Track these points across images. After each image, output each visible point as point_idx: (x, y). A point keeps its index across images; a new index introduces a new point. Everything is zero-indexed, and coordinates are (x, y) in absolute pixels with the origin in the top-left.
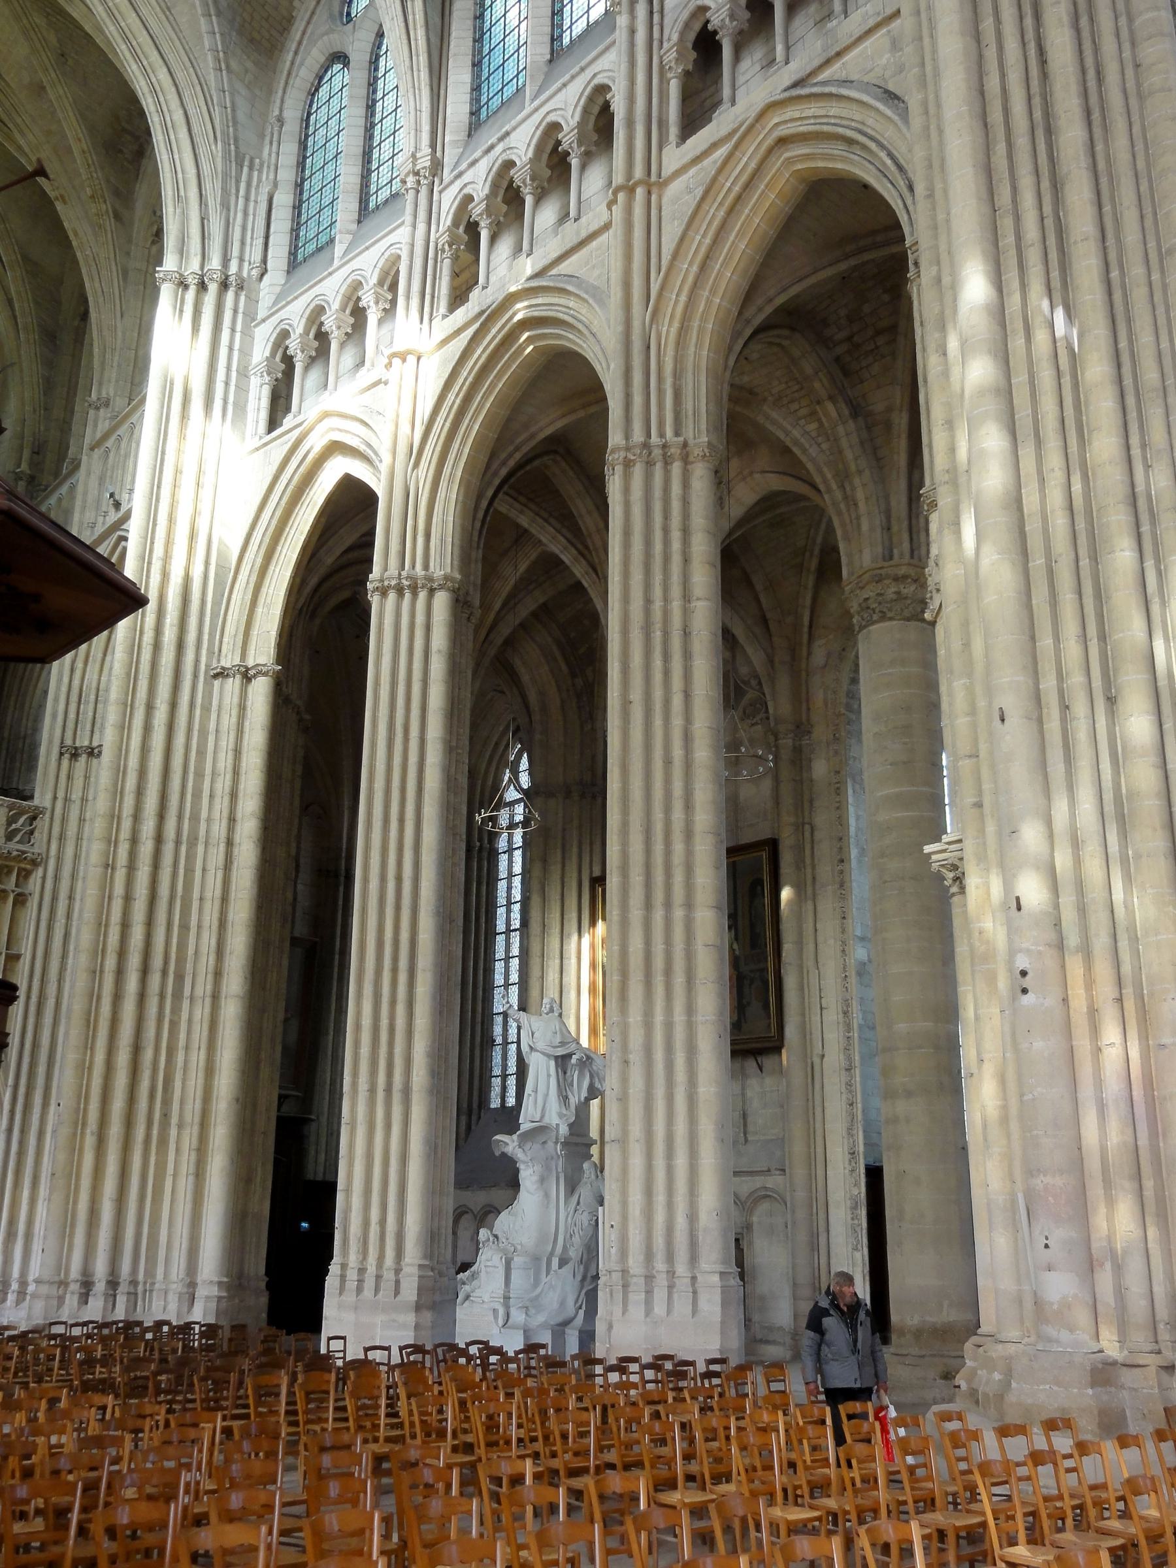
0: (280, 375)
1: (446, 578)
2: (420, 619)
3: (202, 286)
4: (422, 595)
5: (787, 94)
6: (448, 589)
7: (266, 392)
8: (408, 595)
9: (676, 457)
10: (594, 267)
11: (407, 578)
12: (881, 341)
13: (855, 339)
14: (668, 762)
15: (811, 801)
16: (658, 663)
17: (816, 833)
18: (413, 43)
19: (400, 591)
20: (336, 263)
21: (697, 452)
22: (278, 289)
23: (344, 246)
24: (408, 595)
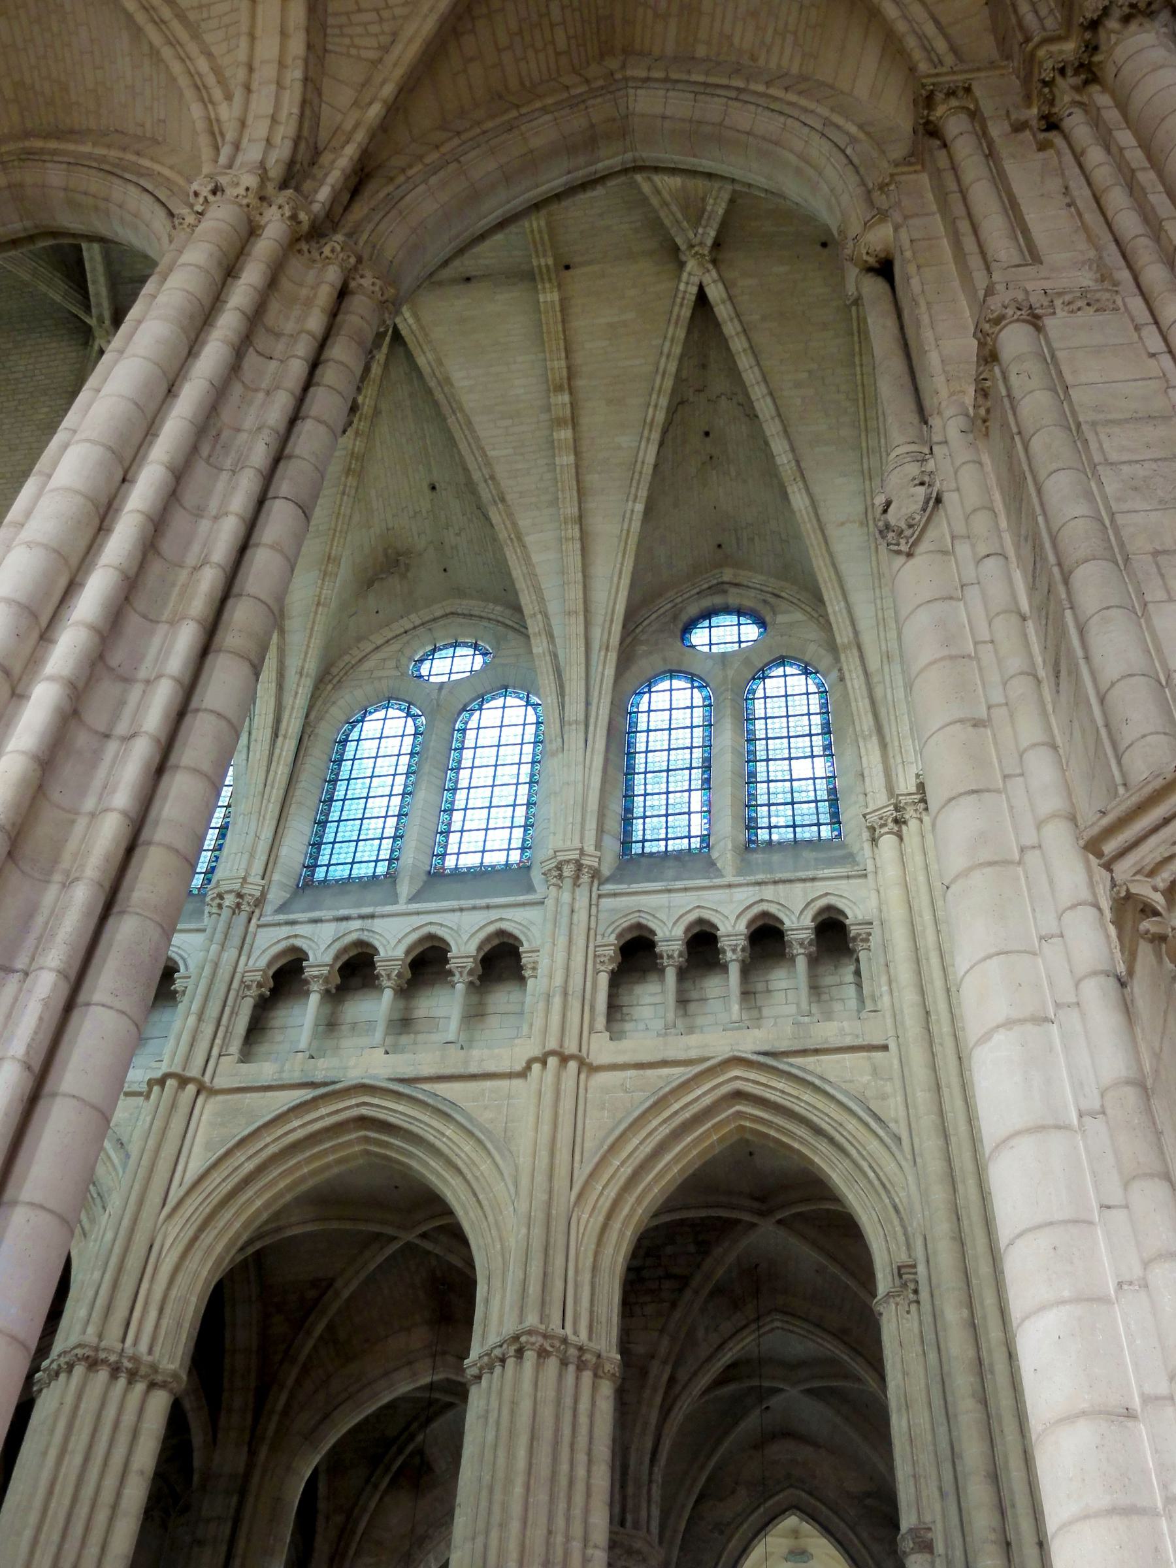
1: (175, 1376)
2: (129, 1418)
4: (140, 1387)
5: (755, 1057)
6: (171, 1391)
9: (590, 1365)
10: (486, 1108)
11: (130, 1359)
12: (667, 1284)
18: (271, 773)
19: (115, 1371)
21: (608, 1367)
24: (122, 1381)
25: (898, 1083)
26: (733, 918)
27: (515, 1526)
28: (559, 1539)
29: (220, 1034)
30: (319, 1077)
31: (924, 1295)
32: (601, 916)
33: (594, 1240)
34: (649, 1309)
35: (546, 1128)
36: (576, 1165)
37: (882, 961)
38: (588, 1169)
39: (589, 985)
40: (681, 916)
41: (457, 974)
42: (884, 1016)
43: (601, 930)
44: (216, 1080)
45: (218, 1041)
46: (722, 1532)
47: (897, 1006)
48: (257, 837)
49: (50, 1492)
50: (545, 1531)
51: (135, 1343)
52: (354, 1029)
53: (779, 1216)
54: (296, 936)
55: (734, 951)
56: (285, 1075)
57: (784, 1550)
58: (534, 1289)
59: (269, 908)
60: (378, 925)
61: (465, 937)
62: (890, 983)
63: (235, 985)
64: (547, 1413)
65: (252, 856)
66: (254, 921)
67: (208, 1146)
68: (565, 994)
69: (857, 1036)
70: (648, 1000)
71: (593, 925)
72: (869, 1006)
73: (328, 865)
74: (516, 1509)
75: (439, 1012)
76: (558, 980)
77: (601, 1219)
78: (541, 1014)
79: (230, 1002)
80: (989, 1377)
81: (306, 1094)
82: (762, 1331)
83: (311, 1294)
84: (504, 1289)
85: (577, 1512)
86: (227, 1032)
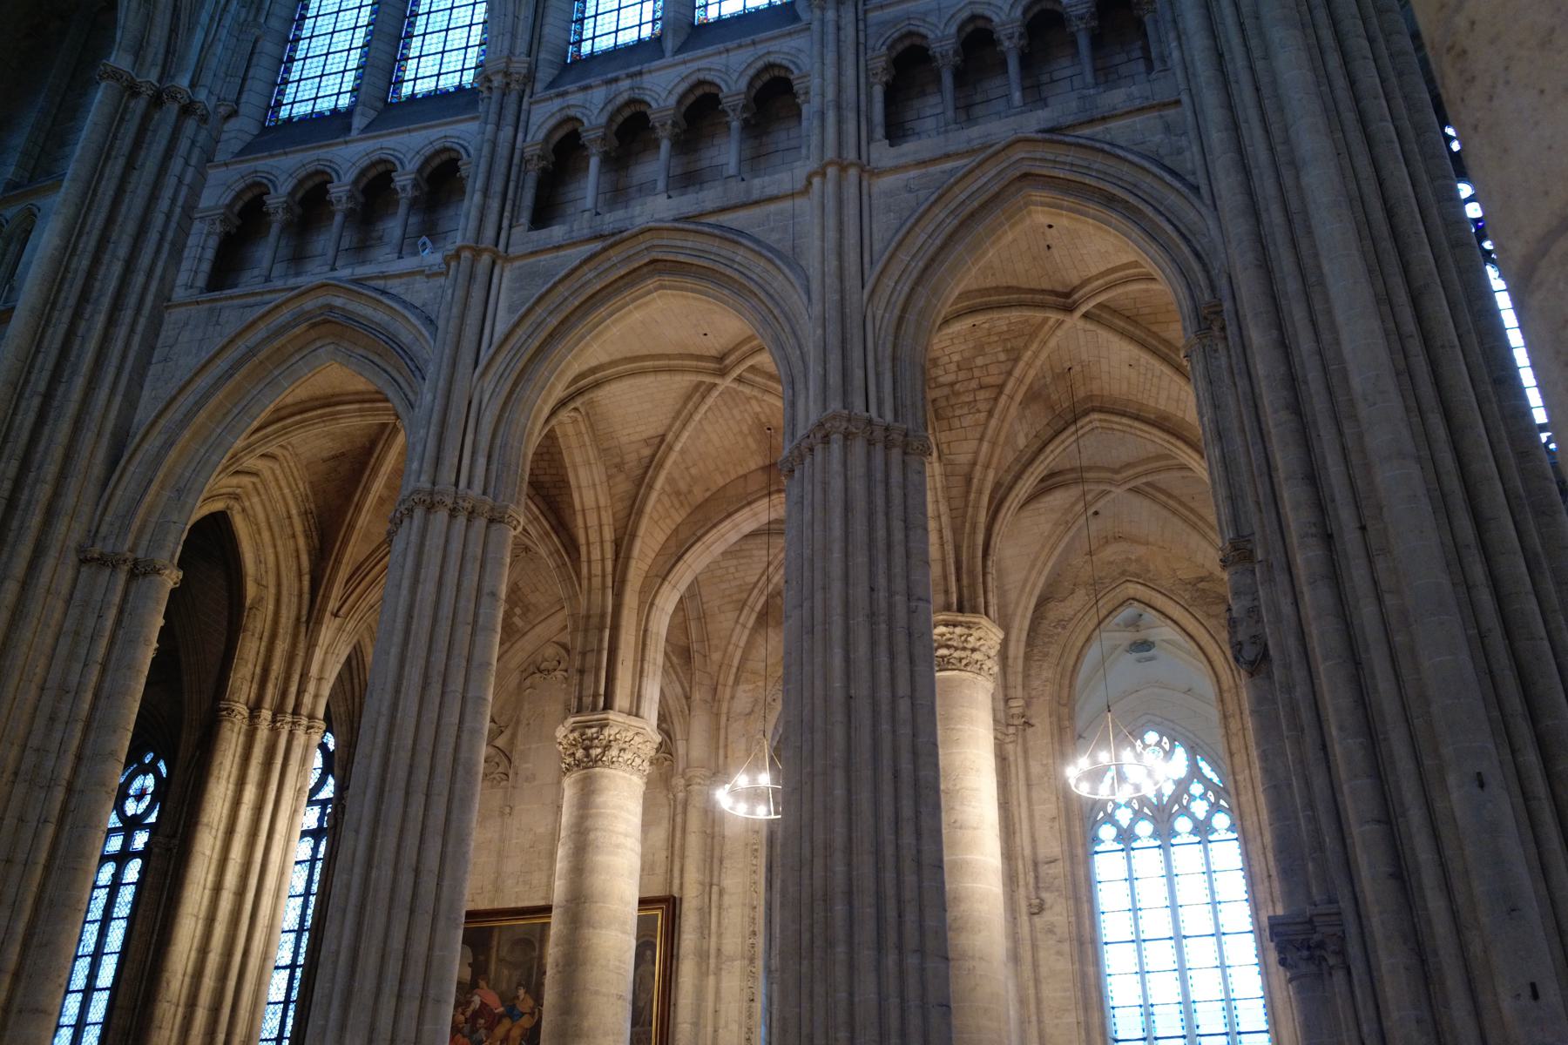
0: (234, 231)
3: (157, 101)
5: (1040, 136)
7: (213, 242)
8: (461, 520)
10: (772, 230)
12: (982, 395)
13: (957, 387)
14: (896, 775)
15: (721, 862)
16: (884, 659)
17: (726, 898)
20: (354, 133)
22: (248, 138)
23: (366, 121)
24: (461, 520)
25: (1192, 134)
26: (1006, 8)
27: (837, 587)
28: (882, 595)
29: (508, 207)
30: (607, 229)
31: (1231, 330)
32: (870, 31)
33: (891, 330)
34: (968, 421)
35: (832, 235)
36: (867, 266)
37: (1168, 17)
38: (878, 268)
39: (863, 97)
40: (952, 16)
41: (732, 114)
42: (1174, 74)
43: (871, 43)
44: (510, 250)
45: (507, 214)
46: (1064, 627)
47: (1188, 59)
48: (516, 17)
49: (410, 616)
50: (867, 589)
51: (469, 485)
52: (640, 191)
53: (1084, 309)
54: (568, 107)
55: (1010, 38)
56: (574, 234)
57: (1126, 643)
58: (834, 379)
59: (539, 87)
60: (647, 80)
61: (735, 77)
62: (1179, 38)
63: (516, 160)
64: (858, 487)
65: (514, 36)
66: (526, 99)
67: (511, 309)
68: (839, 107)
69: (1147, 98)
70: (929, 112)
71: (862, 40)
72: (1158, 65)
73: (593, 38)
74: (836, 570)
75: (721, 160)
76: (830, 95)
77: (897, 312)
78: (817, 131)
79: (513, 177)
80: (1303, 387)
81: (597, 246)
82: (1080, 433)
83: (647, 452)
84: (807, 389)
85: (898, 569)
86: (514, 205)
